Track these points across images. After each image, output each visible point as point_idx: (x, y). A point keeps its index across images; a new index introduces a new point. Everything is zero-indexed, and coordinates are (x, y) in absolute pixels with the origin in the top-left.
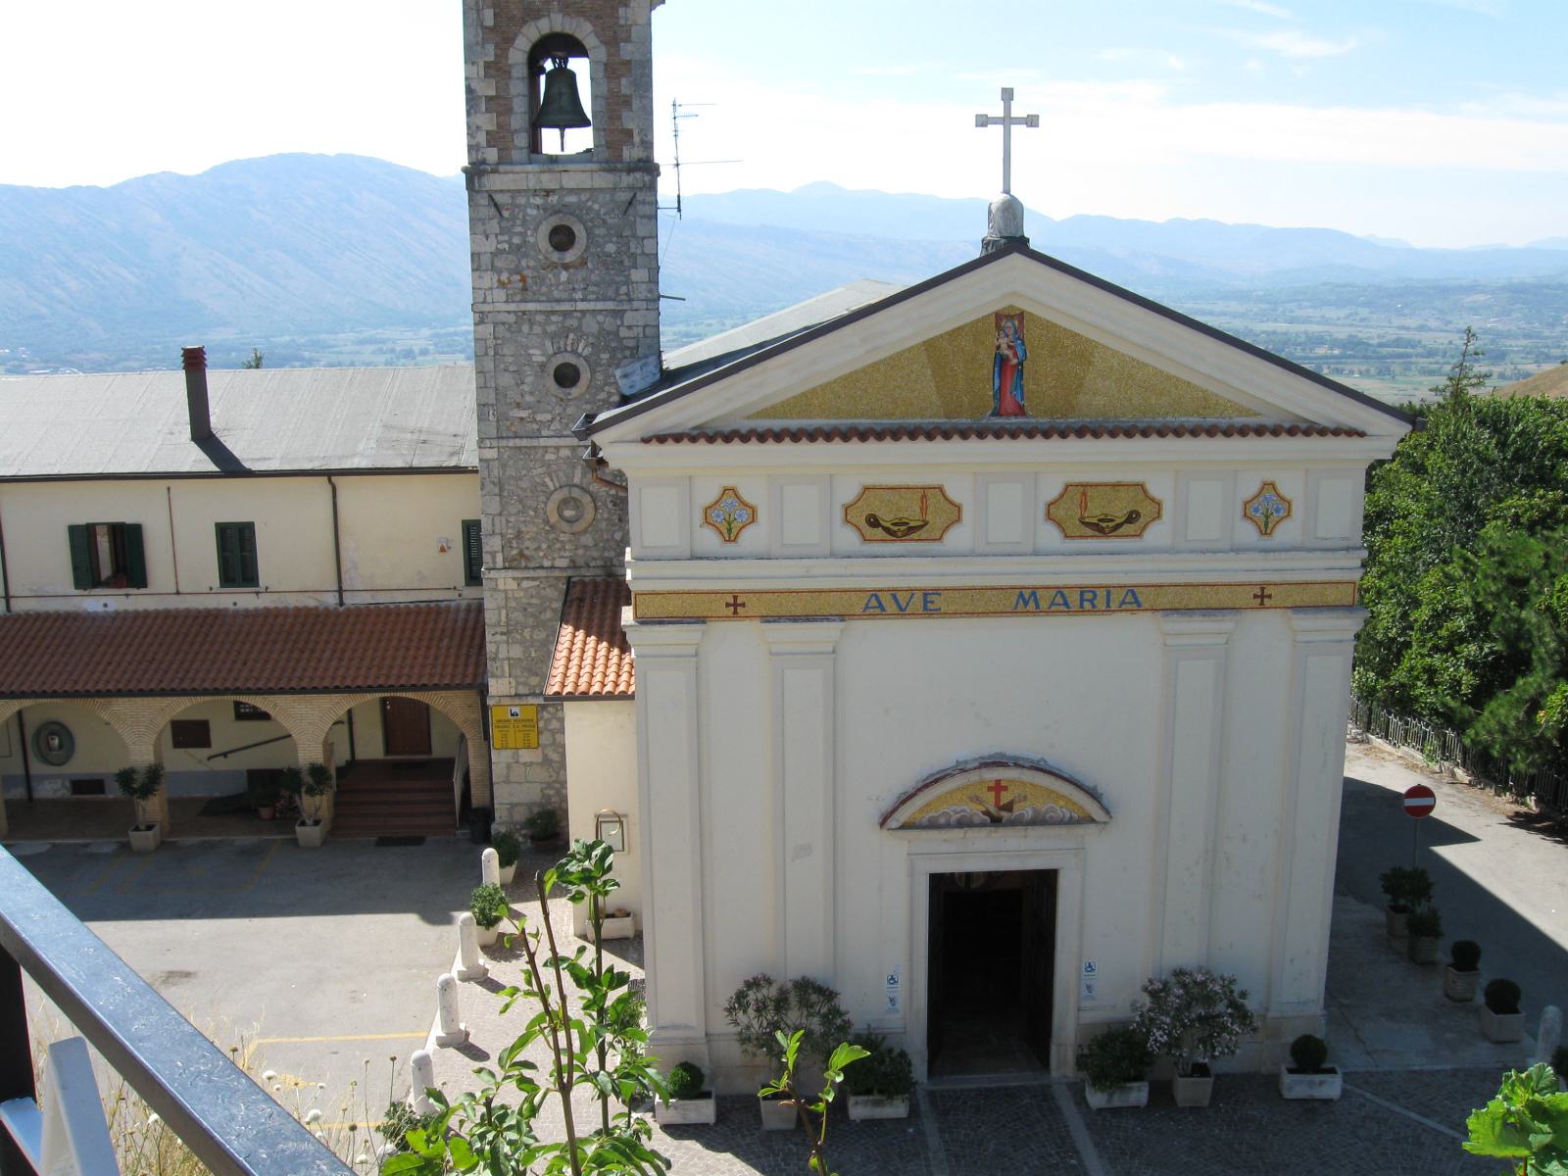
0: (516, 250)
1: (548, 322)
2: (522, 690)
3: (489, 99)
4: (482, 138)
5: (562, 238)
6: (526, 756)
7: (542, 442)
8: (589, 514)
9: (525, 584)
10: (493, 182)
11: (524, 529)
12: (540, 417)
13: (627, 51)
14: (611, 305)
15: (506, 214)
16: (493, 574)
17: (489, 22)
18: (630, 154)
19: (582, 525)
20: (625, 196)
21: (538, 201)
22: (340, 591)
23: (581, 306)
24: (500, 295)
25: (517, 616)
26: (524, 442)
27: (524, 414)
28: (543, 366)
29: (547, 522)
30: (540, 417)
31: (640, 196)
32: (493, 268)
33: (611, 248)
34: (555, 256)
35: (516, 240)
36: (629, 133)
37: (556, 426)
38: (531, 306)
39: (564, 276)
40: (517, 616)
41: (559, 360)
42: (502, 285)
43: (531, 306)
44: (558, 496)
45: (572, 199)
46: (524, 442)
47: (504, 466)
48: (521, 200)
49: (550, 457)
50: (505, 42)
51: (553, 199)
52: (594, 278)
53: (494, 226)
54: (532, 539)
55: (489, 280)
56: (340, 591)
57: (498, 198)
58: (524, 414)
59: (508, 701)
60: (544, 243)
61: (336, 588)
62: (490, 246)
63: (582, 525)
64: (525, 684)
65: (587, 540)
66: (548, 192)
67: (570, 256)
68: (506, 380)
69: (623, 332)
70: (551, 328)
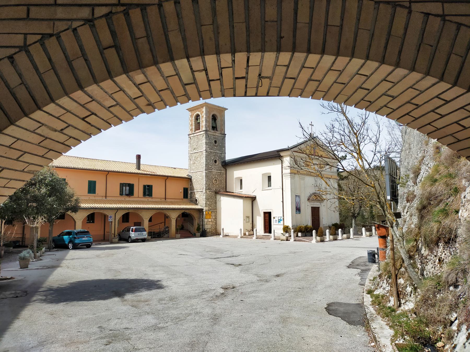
0: (210, 143)
1: (214, 154)
2: (209, 209)
4: (207, 126)
5: (216, 142)
6: (210, 220)
7: (213, 171)
8: (218, 182)
9: (210, 192)
10: (209, 133)
12: (212, 167)
14: (221, 152)
18: (223, 132)
19: (217, 184)
20: (222, 138)
22: (165, 198)
23: (218, 152)
24: (208, 149)
25: (209, 197)
26: (211, 171)
27: (211, 166)
28: (213, 160)
29: (213, 183)
30: (212, 167)
31: (224, 138)
32: (208, 145)
33: (221, 144)
34: (215, 144)
37: (214, 169)
38: (212, 151)
39: (216, 147)
40: (209, 197)
41: (215, 159)
42: (209, 147)
43: (212, 151)
44: (214, 179)
45: (217, 137)
46: (211, 171)
47: (208, 174)
49: (213, 173)
50: (210, 114)
52: (219, 148)
53: (208, 139)
54: (211, 185)
55: (207, 146)
58: (211, 166)
59: (207, 211)
60: (214, 143)
61: (164, 197)
62: (207, 141)
63: (217, 184)
64: (210, 208)
65: (217, 186)
67: (216, 145)
68: (209, 161)
69: (222, 157)
70: (214, 155)
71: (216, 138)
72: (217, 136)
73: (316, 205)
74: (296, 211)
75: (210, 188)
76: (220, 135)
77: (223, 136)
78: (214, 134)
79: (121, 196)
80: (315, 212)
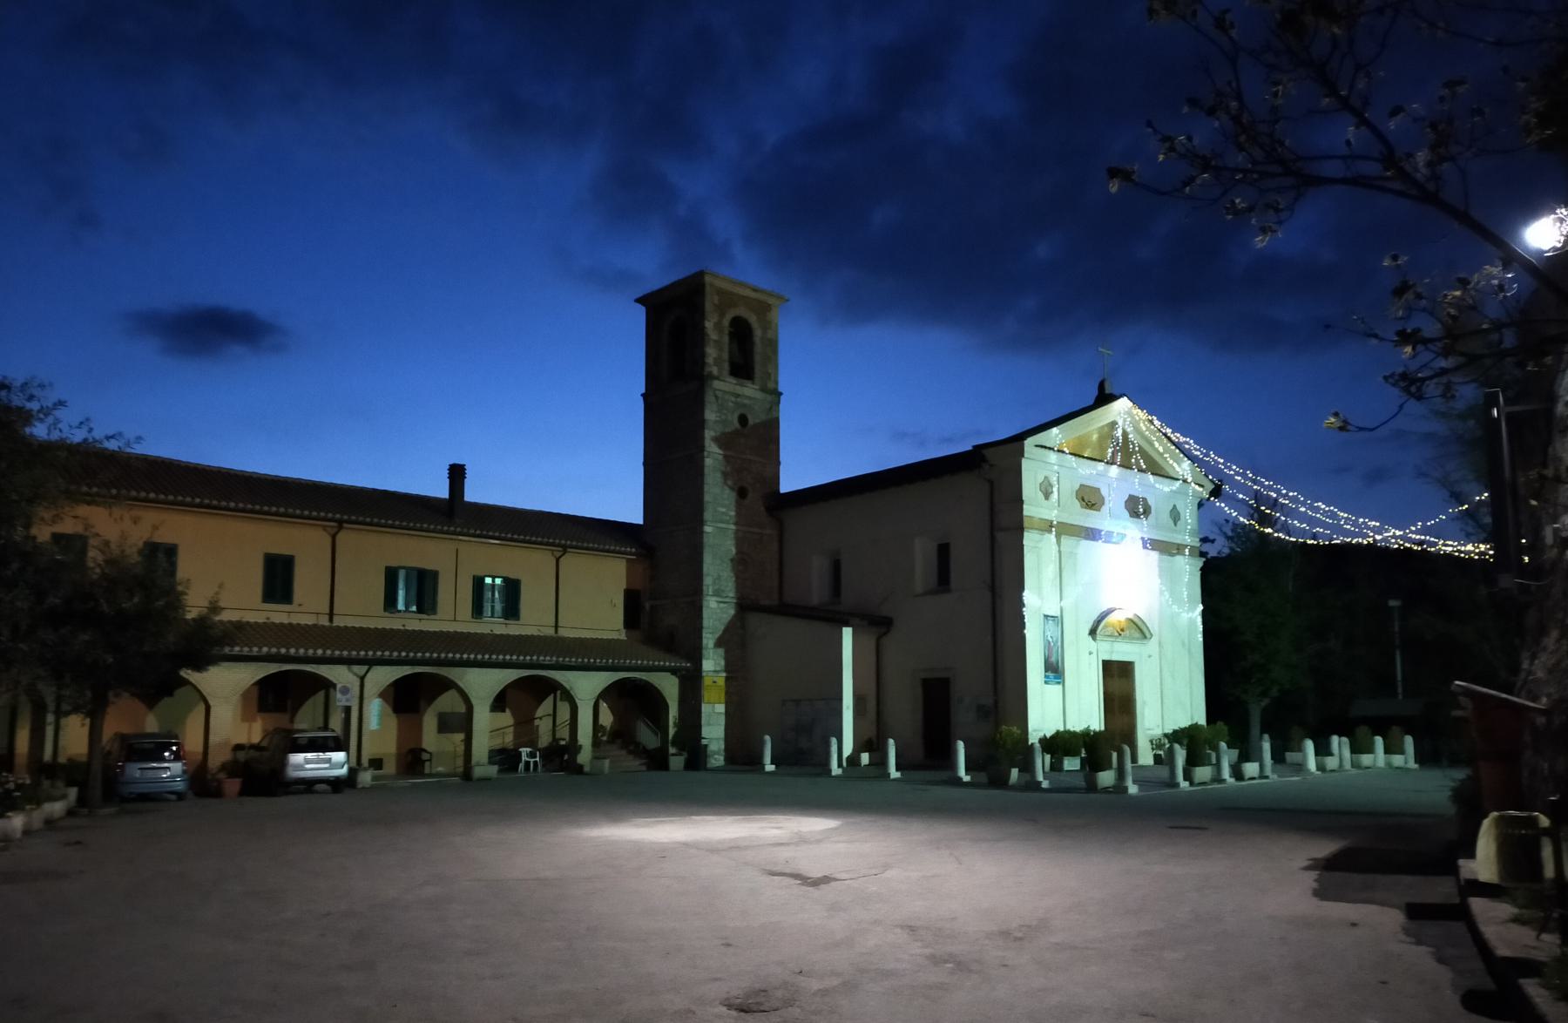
2: (718, 669)
3: (715, 341)
9: (722, 605)
11: (721, 574)
13: (770, 334)
15: (720, 401)
16: (709, 598)
17: (716, 302)
21: (733, 399)
27: (724, 510)
35: (723, 417)
36: (769, 374)
45: (746, 401)
48: (727, 397)
51: (739, 400)
56: (556, 627)
57: (717, 392)
58: (724, 510)
59: (711, 674)
66: (738, 396)
71: (744, 406)
72: (750, 398)
73: (1121, 651)
74: (1046, 676)
75: (723, 591)
76: (759, 395)
77: (769, 398)
78: (739, 390)
79: (387, 614)
80: (1118, 677)
